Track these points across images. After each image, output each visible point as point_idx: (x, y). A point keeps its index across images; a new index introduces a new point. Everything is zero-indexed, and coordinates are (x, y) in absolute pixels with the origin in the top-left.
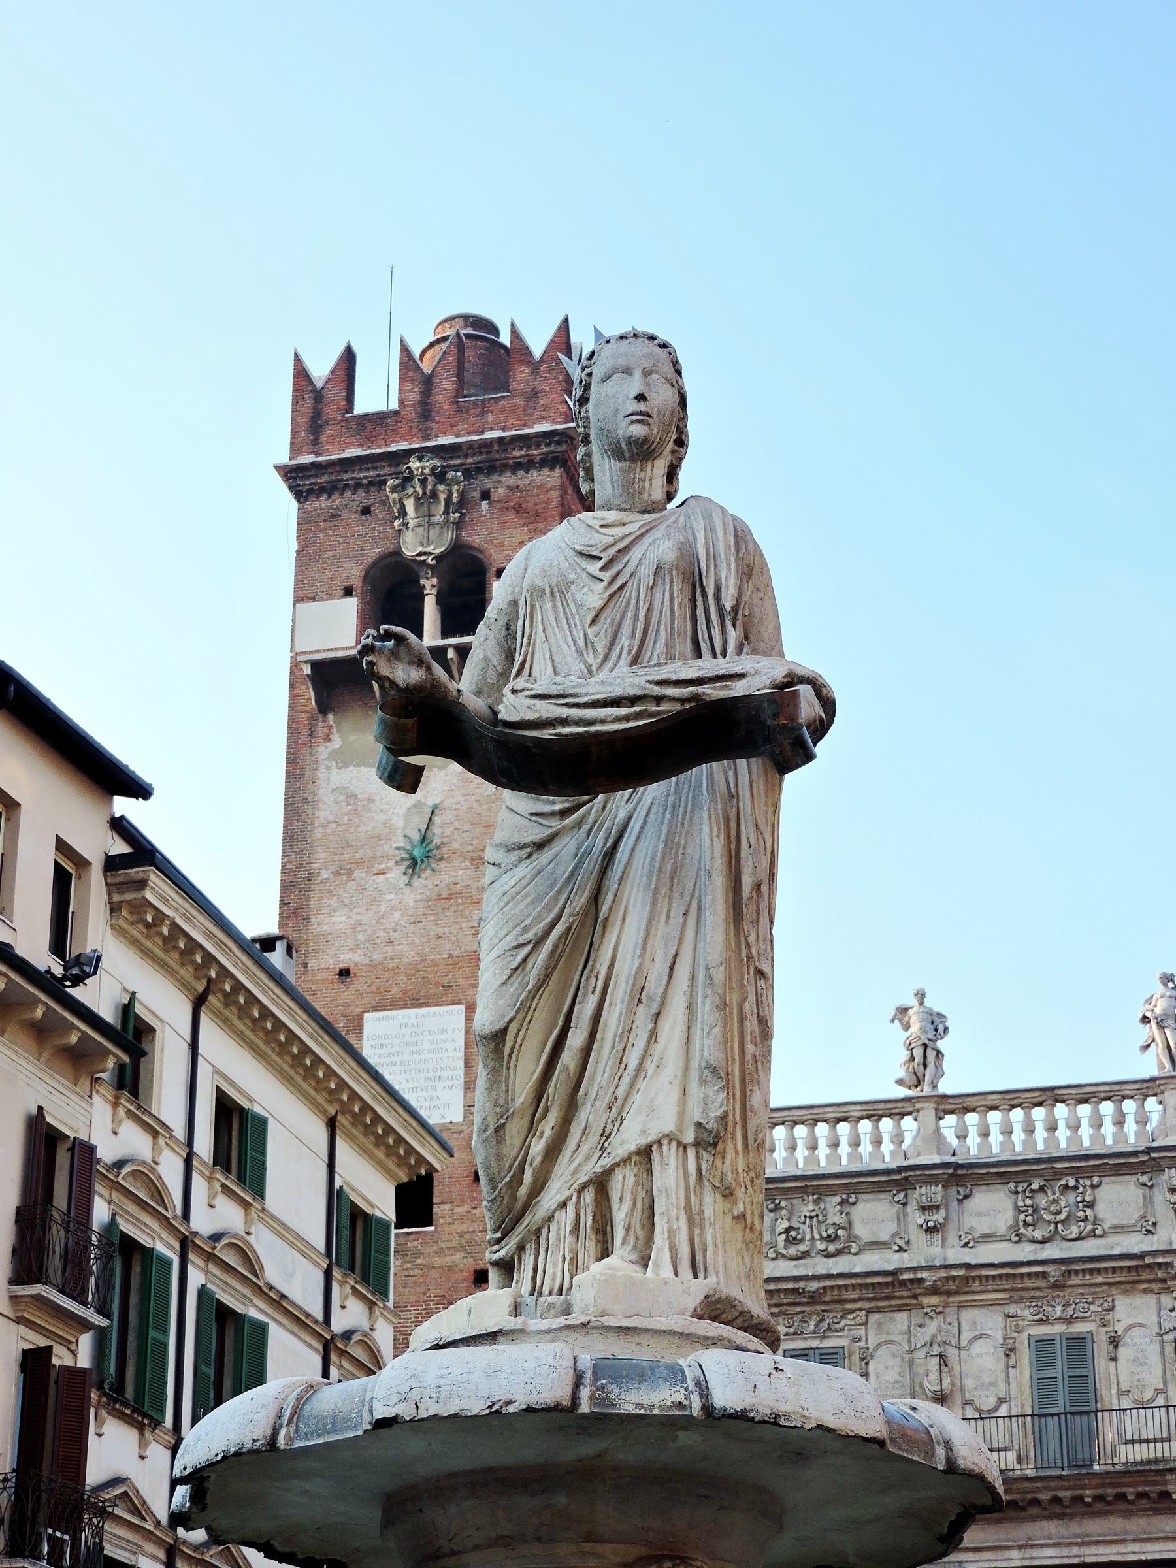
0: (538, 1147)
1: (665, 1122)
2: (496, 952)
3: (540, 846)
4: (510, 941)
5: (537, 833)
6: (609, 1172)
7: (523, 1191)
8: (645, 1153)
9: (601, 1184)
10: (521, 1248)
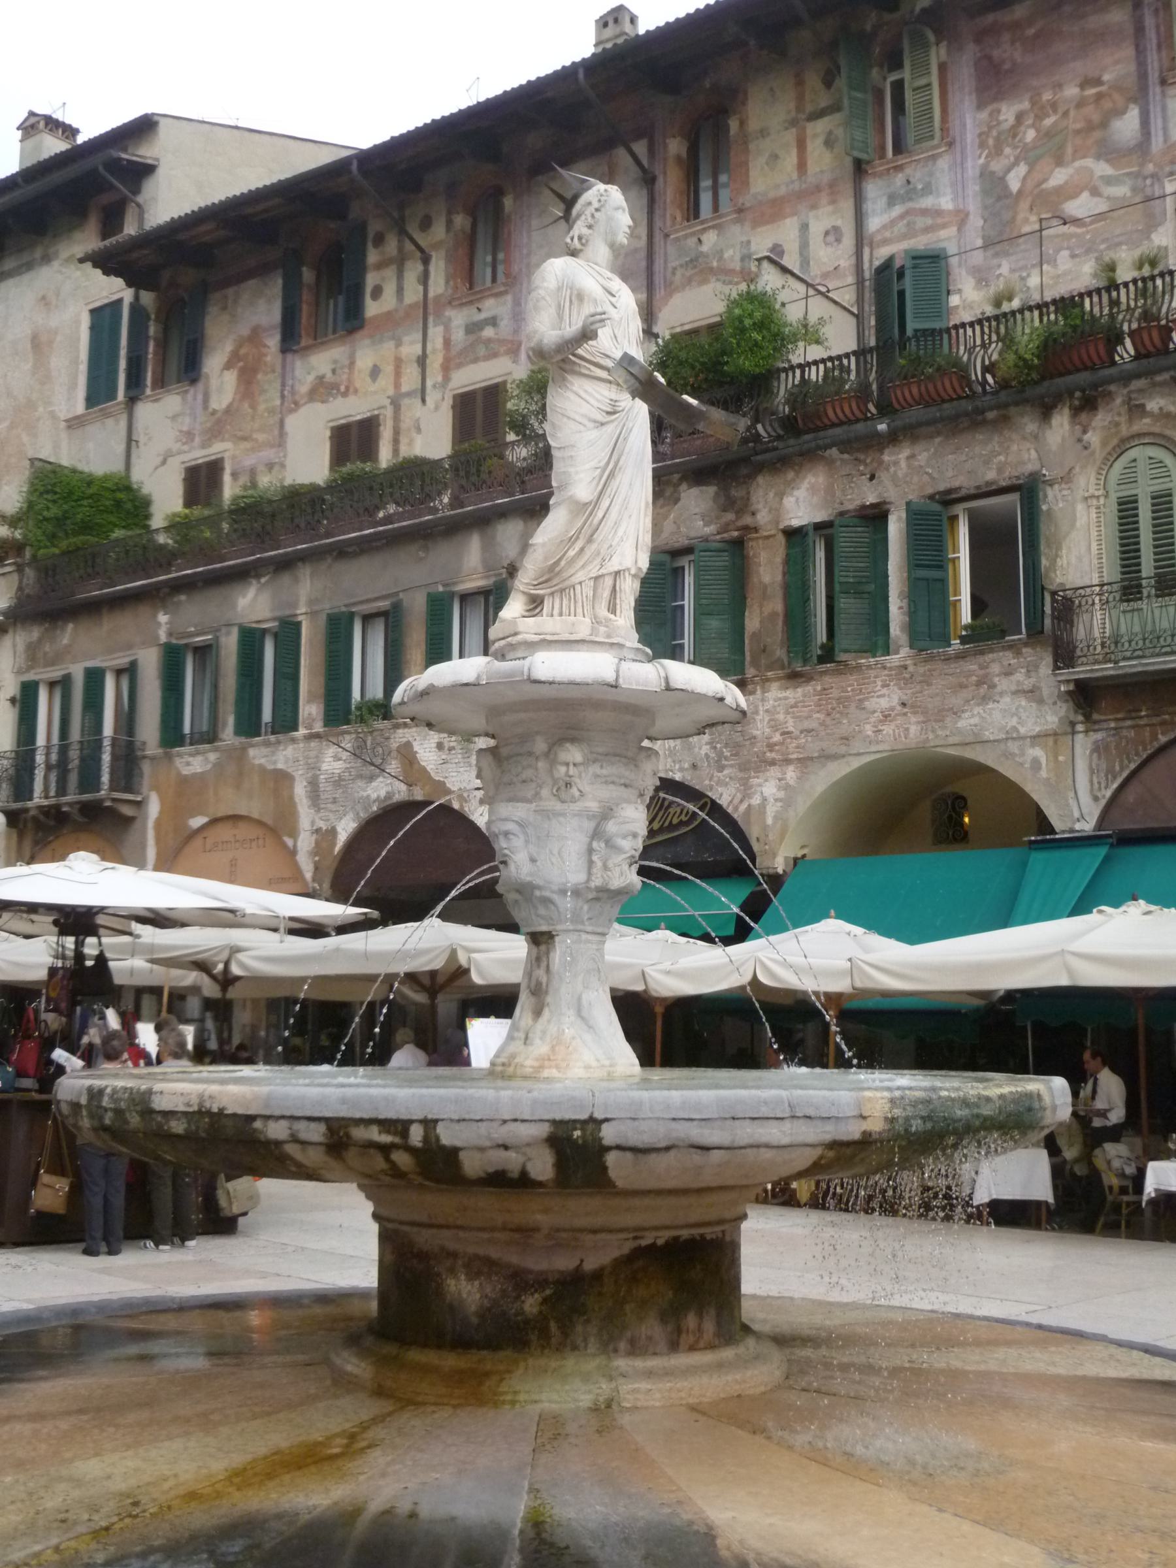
0: (571, 553)
1: (628, 562)
2: (587, 466)
3: (602, 424)
4: (593, 464)
5: (600, 417)
6: (603, 576)
7: (557, 569)
8: (617, 573)
9: (596, 578)
10: (552, 594)
